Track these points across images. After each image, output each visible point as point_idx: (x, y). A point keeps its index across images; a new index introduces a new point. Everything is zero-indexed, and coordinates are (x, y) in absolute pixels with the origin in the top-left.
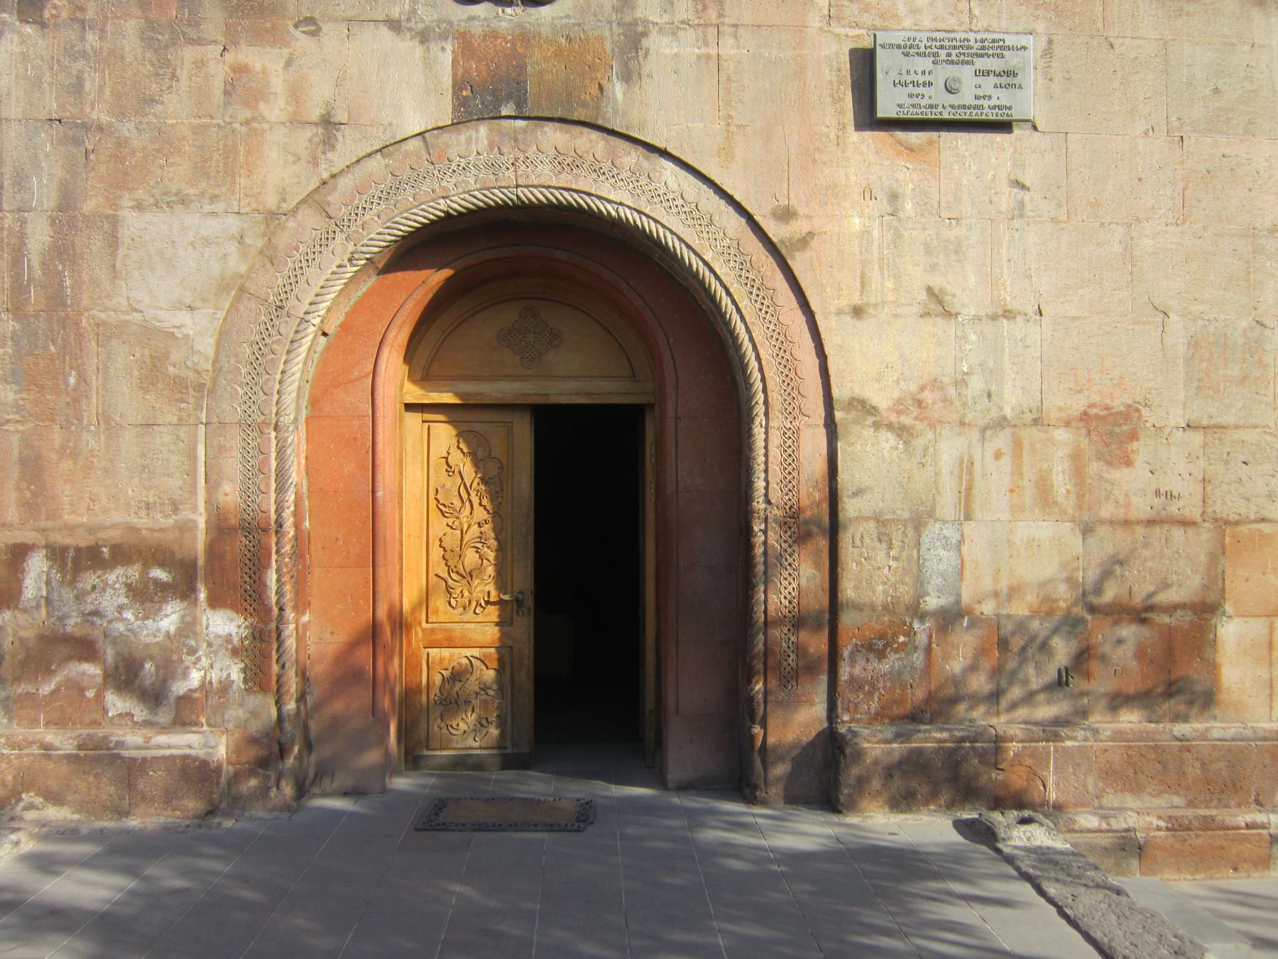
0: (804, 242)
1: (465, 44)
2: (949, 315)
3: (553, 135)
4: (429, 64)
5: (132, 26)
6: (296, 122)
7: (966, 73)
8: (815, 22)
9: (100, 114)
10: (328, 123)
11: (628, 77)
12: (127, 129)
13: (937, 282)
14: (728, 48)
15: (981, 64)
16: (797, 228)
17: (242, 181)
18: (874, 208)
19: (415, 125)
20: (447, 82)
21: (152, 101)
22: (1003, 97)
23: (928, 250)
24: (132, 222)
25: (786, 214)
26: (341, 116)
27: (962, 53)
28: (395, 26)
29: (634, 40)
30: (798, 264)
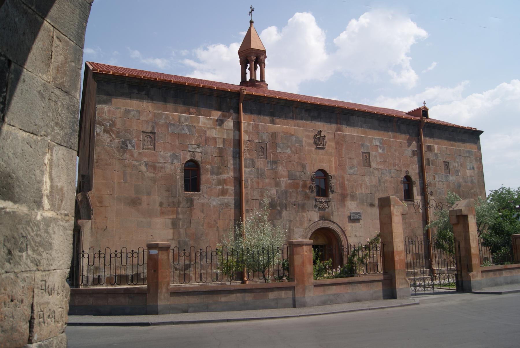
0: (346, 231)
1: (320, 213)
2: (357, 237)
3: (327, 222)
4: (317, 215)
5: (294, 211)
6: (307, 220)
7: (357, 215)
8: (346, 211)
9: (292, 219)
10: (310, 220)
11: (332, 216)
12: (294, 221)
13: (356, 234)
14: (340, 213)
15: (359, 215)
16: (345, 229)
17: (303, 226)
18: (351, 227)
19: (316, 220)
20: (319, 216)
21: (296, 218)
22: (360, 217)
23: (355, 231)
24: (295, 229)
25: (344, 228)
26: (311, 219)
27: (357, 213)
28: (314, 211)
29: (332, 212)
30: (345, 232)
